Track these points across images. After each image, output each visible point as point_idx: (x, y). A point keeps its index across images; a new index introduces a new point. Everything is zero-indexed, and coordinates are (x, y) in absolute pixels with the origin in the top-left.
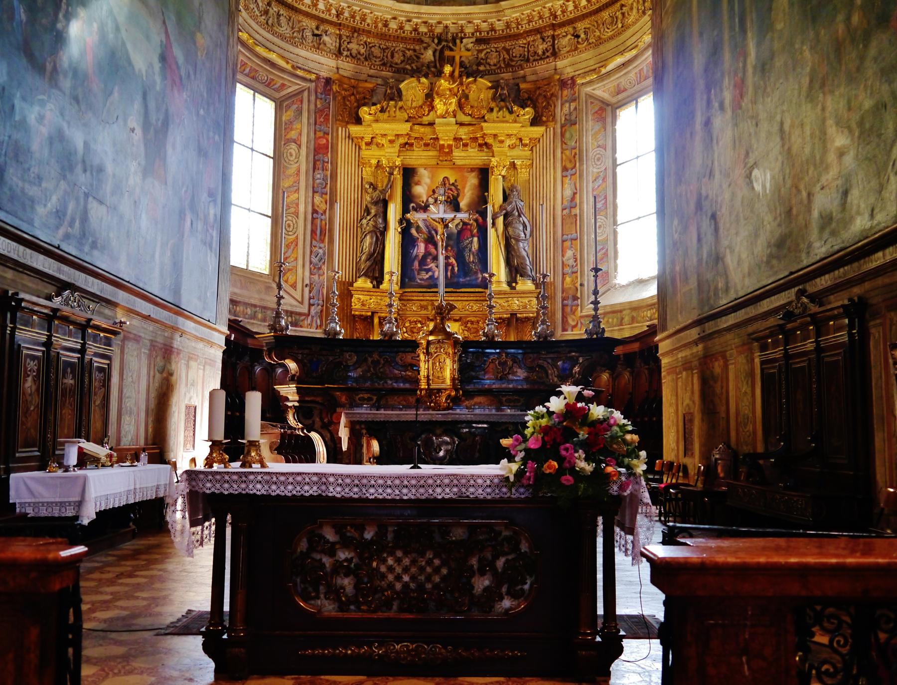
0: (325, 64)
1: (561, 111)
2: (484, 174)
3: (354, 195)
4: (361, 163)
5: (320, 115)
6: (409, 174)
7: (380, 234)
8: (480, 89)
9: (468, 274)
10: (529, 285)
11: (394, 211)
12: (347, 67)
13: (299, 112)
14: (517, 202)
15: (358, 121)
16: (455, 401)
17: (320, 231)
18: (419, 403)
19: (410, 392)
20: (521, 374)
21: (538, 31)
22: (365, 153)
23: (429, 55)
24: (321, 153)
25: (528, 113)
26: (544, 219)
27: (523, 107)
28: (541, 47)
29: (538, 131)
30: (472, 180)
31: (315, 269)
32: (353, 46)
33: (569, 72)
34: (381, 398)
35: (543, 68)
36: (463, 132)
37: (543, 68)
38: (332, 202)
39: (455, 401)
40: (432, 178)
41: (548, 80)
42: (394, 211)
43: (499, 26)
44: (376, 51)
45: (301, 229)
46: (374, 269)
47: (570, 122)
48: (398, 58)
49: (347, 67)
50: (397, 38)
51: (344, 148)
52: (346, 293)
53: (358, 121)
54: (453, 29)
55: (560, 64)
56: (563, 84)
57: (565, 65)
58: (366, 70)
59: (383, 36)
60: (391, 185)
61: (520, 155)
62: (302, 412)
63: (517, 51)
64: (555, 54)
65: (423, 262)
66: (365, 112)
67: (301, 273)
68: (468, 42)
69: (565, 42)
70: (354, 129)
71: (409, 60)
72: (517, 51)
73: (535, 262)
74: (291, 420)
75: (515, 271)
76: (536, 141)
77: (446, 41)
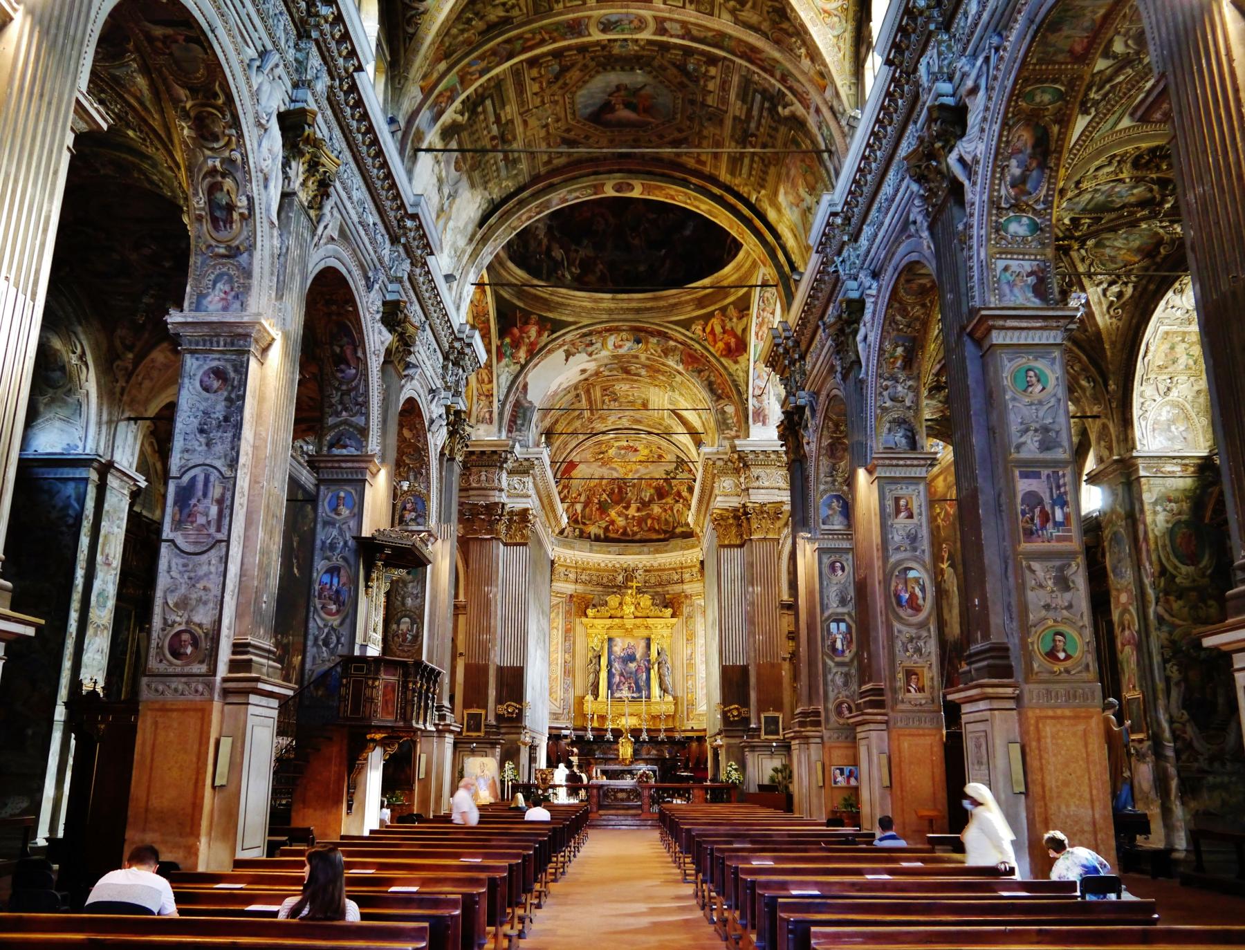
0: (569, 588)
1: (686, 610)
2: (648, 641)
3: (584, 652)
4: (588, 635)
5: (568, 613)
6: (610, 640)
7: (597, 673)
8: (646, 601)
9: (640, 689)
10: (671, 698)
11: (604, 661)
12: (580, 588)
13: (558, 613)
14: (663, 656)
15: (586, 616)
16: (632, 763)
17: (569, 672)
18: (620, 763)
19: (616, 760)
20: (654, 752)
21: (674, 569)
22: (590, 631)
23: (620, 578)
24: (568, 632)
25: (669, 611)
26: (678, 664)
27: (666, 607)
28: (676, 577)
29: (674, 620)
30: (643, 643)
31: (566, 691)
32: (583, 577)
33: (689, 592)
34: (607, 761)
35: (677, 588)
36: (638, 621)
37: (677, 588)
38: (574, 657)
39: (632, 763)
40: (623, 642)
41: (679, 595)
42: (604, 661)
43: (656, 564)
44: (594, 578)
45: (559, 671)
46: (596, 696)
47: (690, 617)
48: (605, 580)
49: (580, 588)
50: (605, 571)
51: (579, 629)
52: (580, 701)
53: (586, 616)
54: (632, 566)
55: (685, 587)
56: (686, 597)
57: (688, 588)
58: (589, 588)
59: (598, 570)
60: (602, 648)
61: (666, 632)
62: (580, 767)
63: (664, 577)
64: (682, 582)
65: (618, 686)
66: (590, 612)
67: (560, 694)
68: (640, 572)
69: (687, 576)
70: (584, 620)
71: (610, 581)
72: (664, 577)
73: (674, 687)
74: (575, 769)
75: (664, 690)
76: (673, 625)
77: (629, 574)
